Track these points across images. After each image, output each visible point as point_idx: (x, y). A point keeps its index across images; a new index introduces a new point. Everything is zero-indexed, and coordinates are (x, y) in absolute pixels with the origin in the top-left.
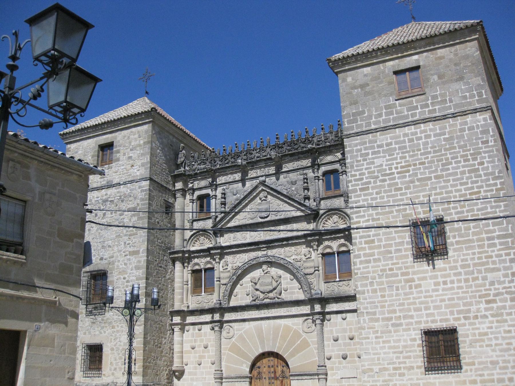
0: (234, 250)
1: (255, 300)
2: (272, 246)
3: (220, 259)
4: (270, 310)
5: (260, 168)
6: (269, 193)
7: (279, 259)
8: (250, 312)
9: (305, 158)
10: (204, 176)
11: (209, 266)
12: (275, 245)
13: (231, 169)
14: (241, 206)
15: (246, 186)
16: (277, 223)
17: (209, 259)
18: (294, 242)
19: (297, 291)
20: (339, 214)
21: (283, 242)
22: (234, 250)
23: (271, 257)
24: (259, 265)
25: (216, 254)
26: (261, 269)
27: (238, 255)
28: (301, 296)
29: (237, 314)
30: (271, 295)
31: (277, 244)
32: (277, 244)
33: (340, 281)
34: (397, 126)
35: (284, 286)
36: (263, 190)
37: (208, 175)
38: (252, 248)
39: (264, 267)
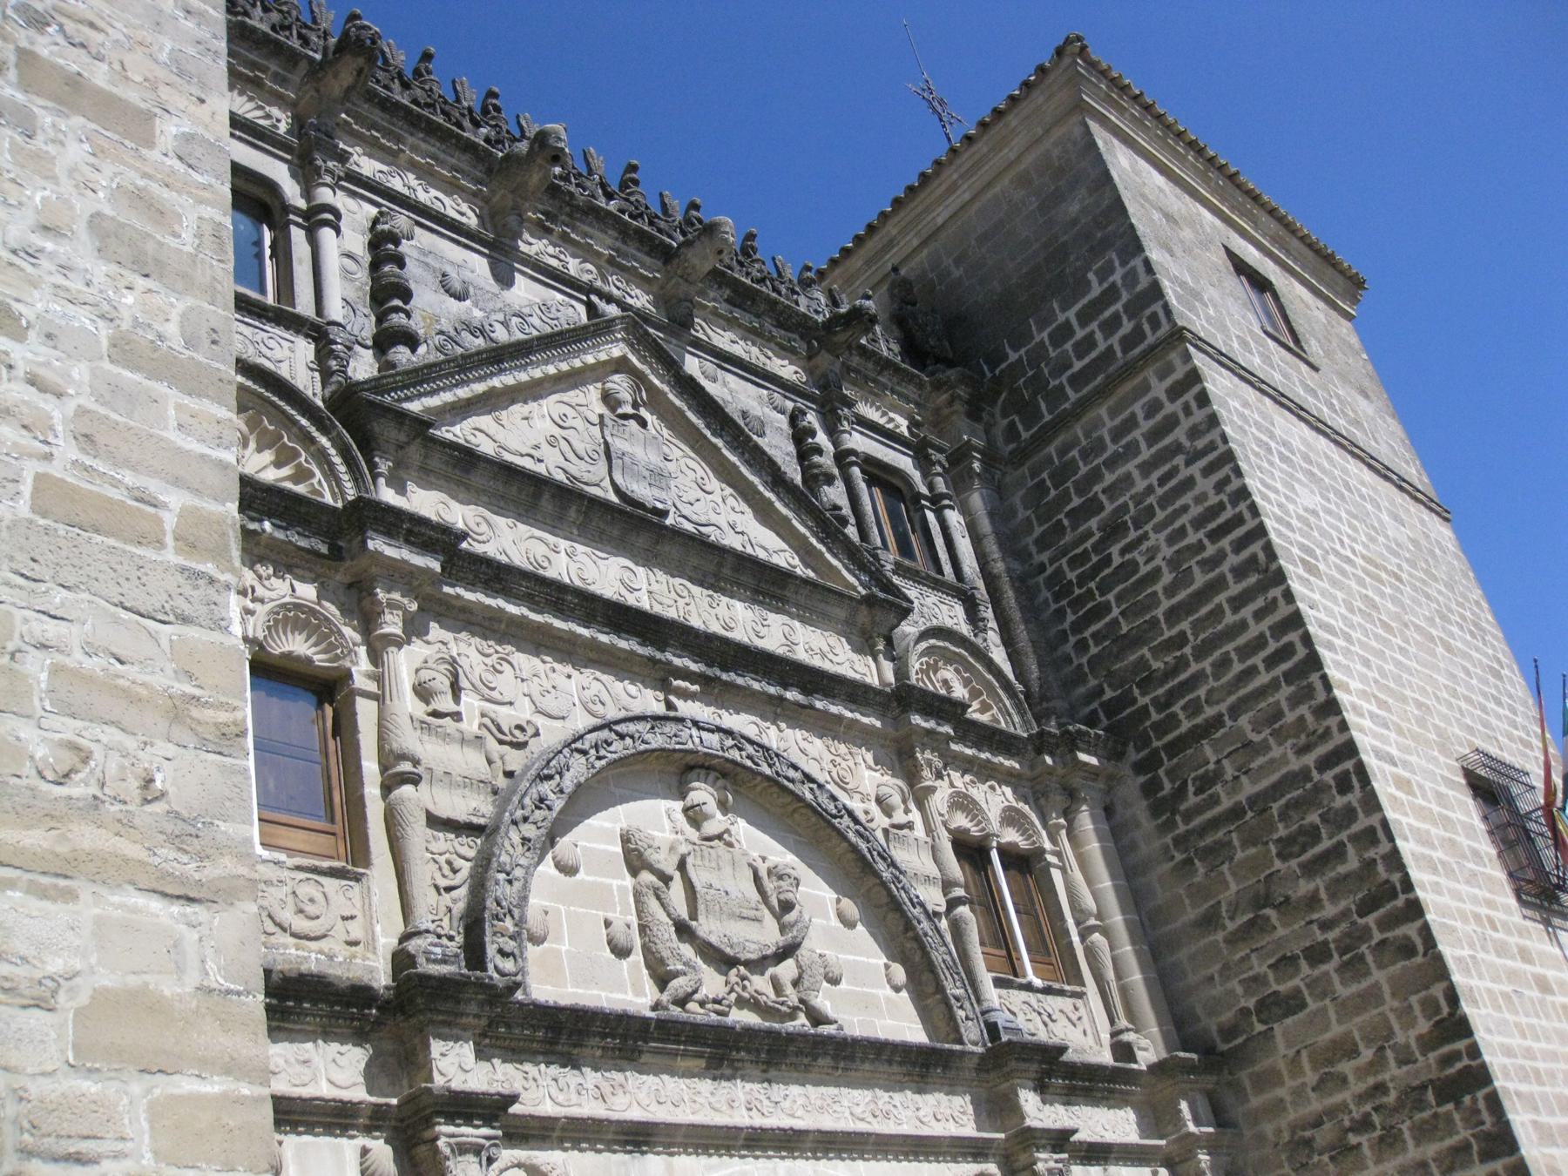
0: (512, 609)
1: (682, 1002)
2: (731, 686)
3: (414, 629)
4: (778, 1090)
5: (586, 253)
6: (656, 402)
7: (791, 773)
8: (671, 1085)
9: (786, 351)
10: (253, 66)
11: (297, 645)
12: (748, 688)
13: (433, 147)
14: (523, 377)
15: (514, 289)
16: (726, 571)
17: (307, 592)
18: (834, 709)
19: (888, 999)
20: (969, 668)
21: (785, 687)
22: (512, 609)
23: (750, 749)
24: (677, 771)
25: (403, 577)
26: (678, 806)
27: (525, 662)
28: (912, 1031)
29: (570, 1076)
30: (760, 984)
31: (756, 686)
32: (756, 686)
33: (1047, 991)
34: (1302, 413)
35: (813, 946)
36: (621, 365)
37: (276, 78)
38: (623, 644)
39: (702, 793)
